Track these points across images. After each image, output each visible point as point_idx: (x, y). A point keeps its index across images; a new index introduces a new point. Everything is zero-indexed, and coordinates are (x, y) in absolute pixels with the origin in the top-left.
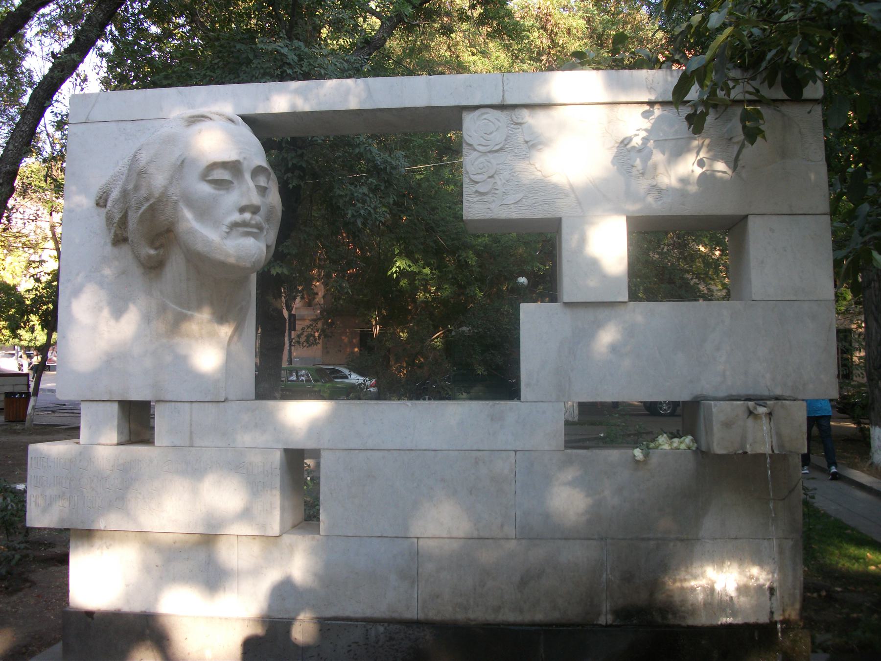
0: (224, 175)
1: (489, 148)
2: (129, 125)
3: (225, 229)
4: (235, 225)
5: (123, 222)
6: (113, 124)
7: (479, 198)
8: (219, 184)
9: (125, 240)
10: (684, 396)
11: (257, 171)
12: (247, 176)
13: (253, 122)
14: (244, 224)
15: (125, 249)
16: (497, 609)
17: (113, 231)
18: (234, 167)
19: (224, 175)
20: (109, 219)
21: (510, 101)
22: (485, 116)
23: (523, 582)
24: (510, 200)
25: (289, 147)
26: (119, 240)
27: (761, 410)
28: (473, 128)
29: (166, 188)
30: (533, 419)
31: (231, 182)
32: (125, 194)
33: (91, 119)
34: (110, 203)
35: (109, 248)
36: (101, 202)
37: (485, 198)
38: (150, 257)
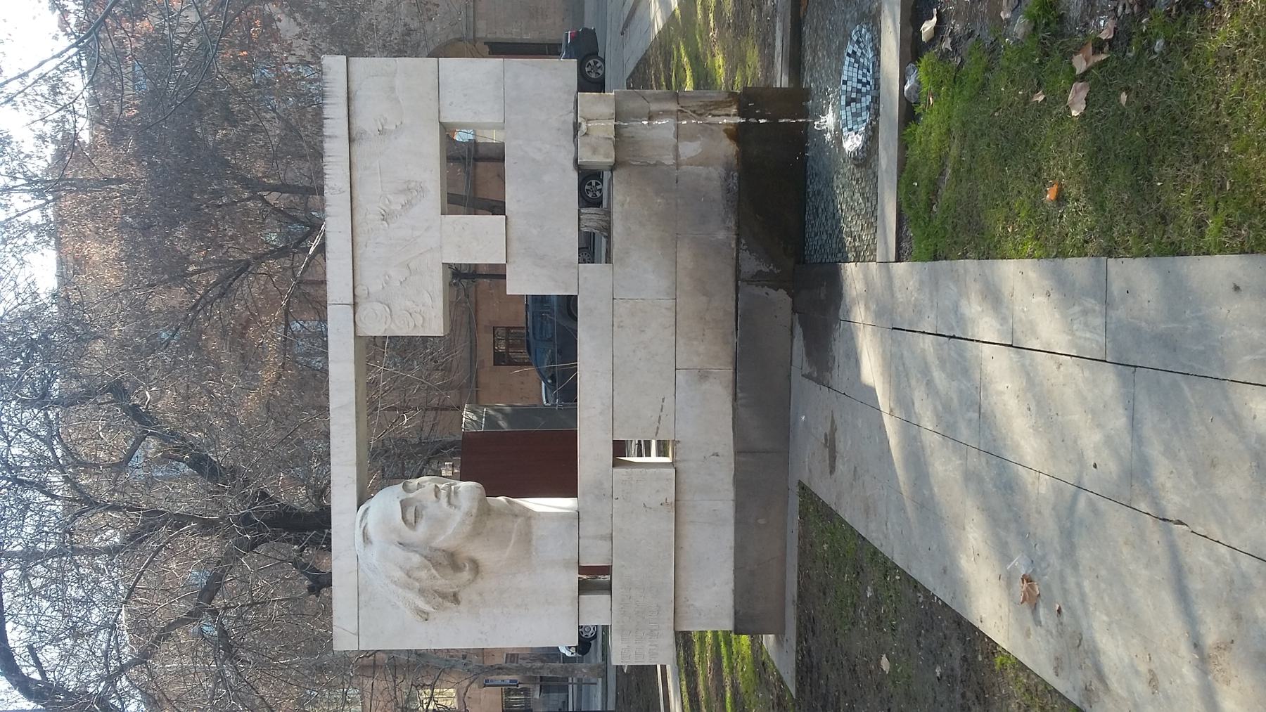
3: (452, 510)
4: (449, 503)
5: (444, 596)
9: (455, 595)
10: (574, 177)
11: (405, 487)
12: (411, 495)
14: (449, 496)
15: (463, 596)
17: (449, 604)
18: (404, 505)
20: (438, 608)
21: (351, 301)
24: (428, 301)
25: (389, 462)
26: (455, 598)
27: (584, 126)
28: (375, 326)
30: (591, 286)
32: (422, 592)
34: (427, 608)
35: (462, 607)
36: (425, 616)
38: (471, 569)
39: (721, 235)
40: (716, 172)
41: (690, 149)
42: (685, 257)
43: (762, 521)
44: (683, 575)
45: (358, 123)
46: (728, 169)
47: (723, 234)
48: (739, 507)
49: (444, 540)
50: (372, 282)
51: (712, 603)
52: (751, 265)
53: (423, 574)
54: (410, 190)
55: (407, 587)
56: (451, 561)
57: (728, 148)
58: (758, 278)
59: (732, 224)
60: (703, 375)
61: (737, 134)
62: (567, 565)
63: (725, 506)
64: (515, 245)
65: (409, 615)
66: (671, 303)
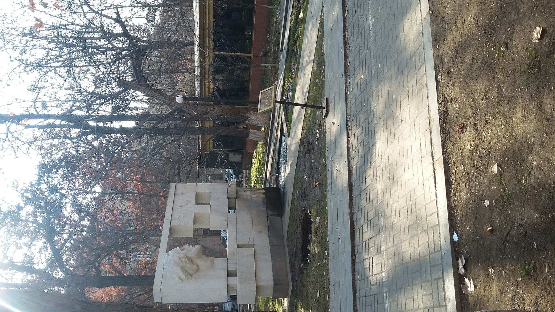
26: (191, 275)
35: (193, 279)
39: (263, 209)
40: (261, 200)
41: (253, 196)
44: (257, 272)
45: (177, 192)
46: (263, 199)
47: (263, 208)
48: (272, 256)
49: (189, 255)
50: (176, 216)
51: (267, 277)
52: (270, 213)
53: (184, 260)
54: (187, 202)
55: (178, 265)
56: (191, 261)
57: (264, 196)
58: (272, 215)
59: (265, 207)
60: (260, 232)
61: (264, 194)
62: (224, 269)
63: (269, 257)
64: (212, 210)
65: (177, 279)
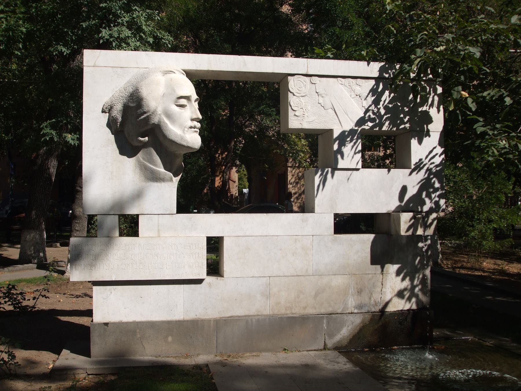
0: (183, 102)
1: (301, 95)
2: (119, 70)
4: (191, 127)
6: (110, 68)
7: (296, 118)
8: (182, 106)
13: (189, 74)
14: (195, 127)
16: (305, 308)
19: (183, 102)
22: (299, 79)
23: (316, 295)
24: (310, 119)
29: (157, 107)
31: (186, 106)
33: (97, 64)
37: (299, 118)
42: (339, 281)
43: (170, 339)
66: (310, 272)
